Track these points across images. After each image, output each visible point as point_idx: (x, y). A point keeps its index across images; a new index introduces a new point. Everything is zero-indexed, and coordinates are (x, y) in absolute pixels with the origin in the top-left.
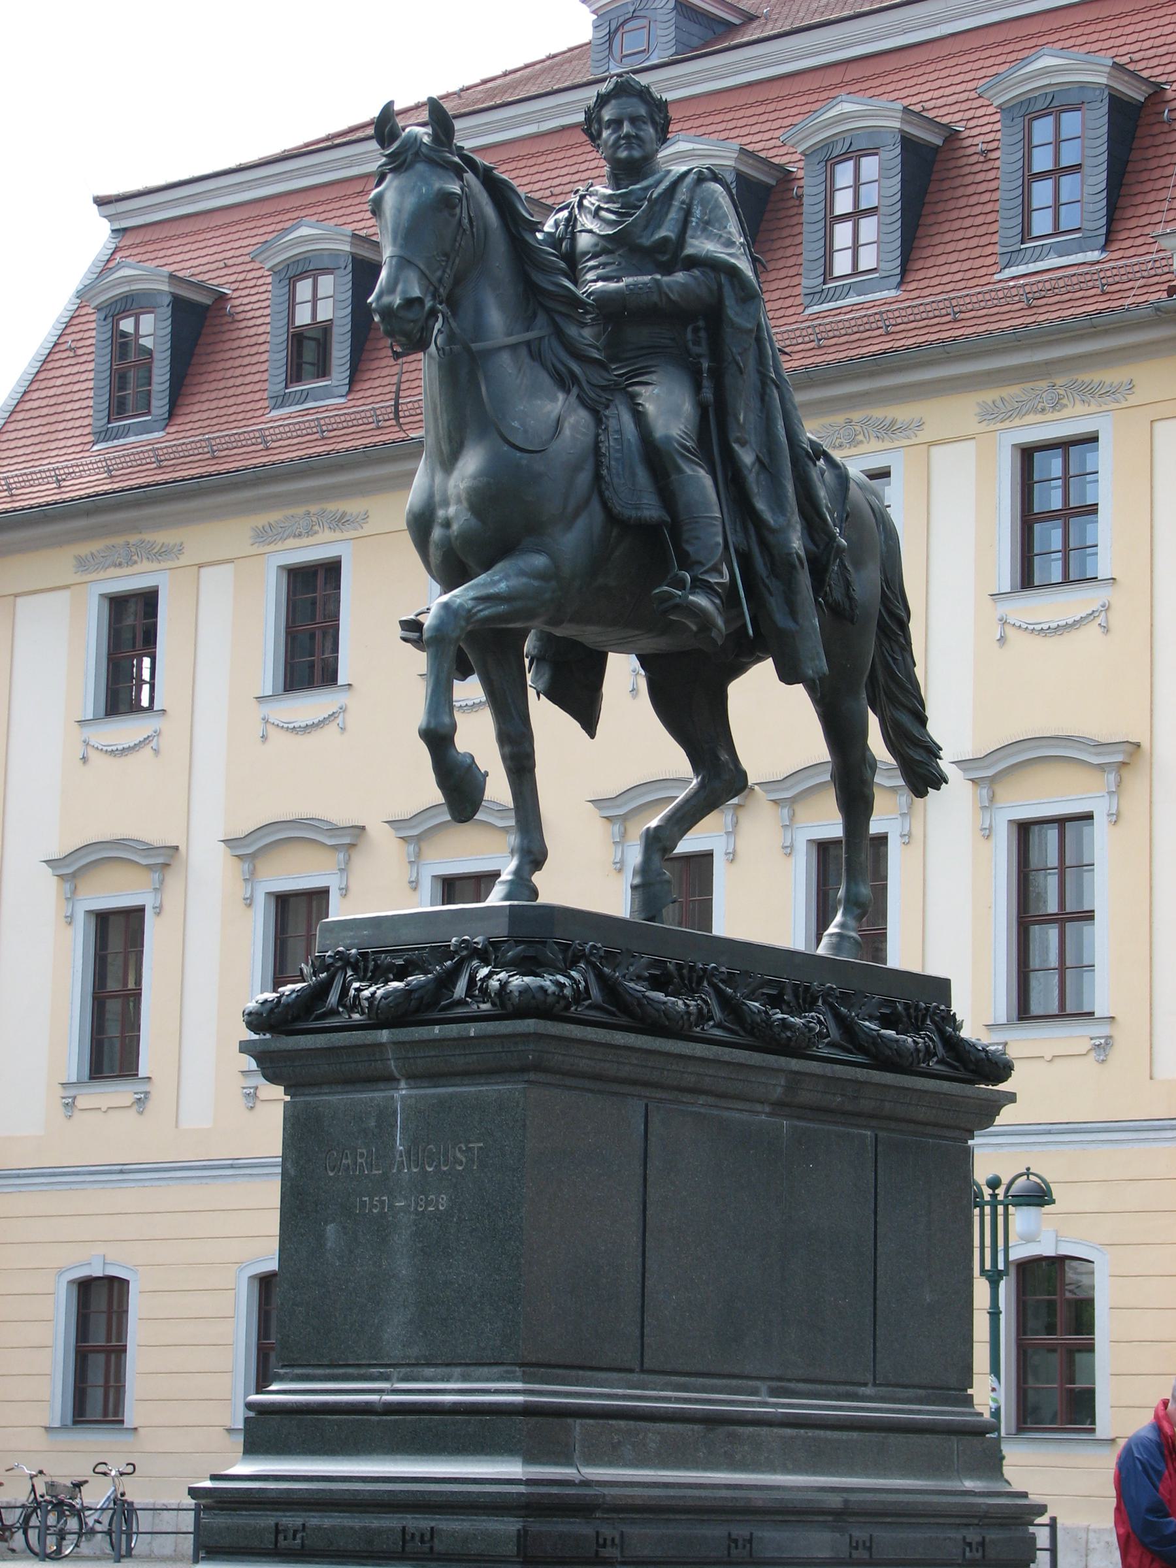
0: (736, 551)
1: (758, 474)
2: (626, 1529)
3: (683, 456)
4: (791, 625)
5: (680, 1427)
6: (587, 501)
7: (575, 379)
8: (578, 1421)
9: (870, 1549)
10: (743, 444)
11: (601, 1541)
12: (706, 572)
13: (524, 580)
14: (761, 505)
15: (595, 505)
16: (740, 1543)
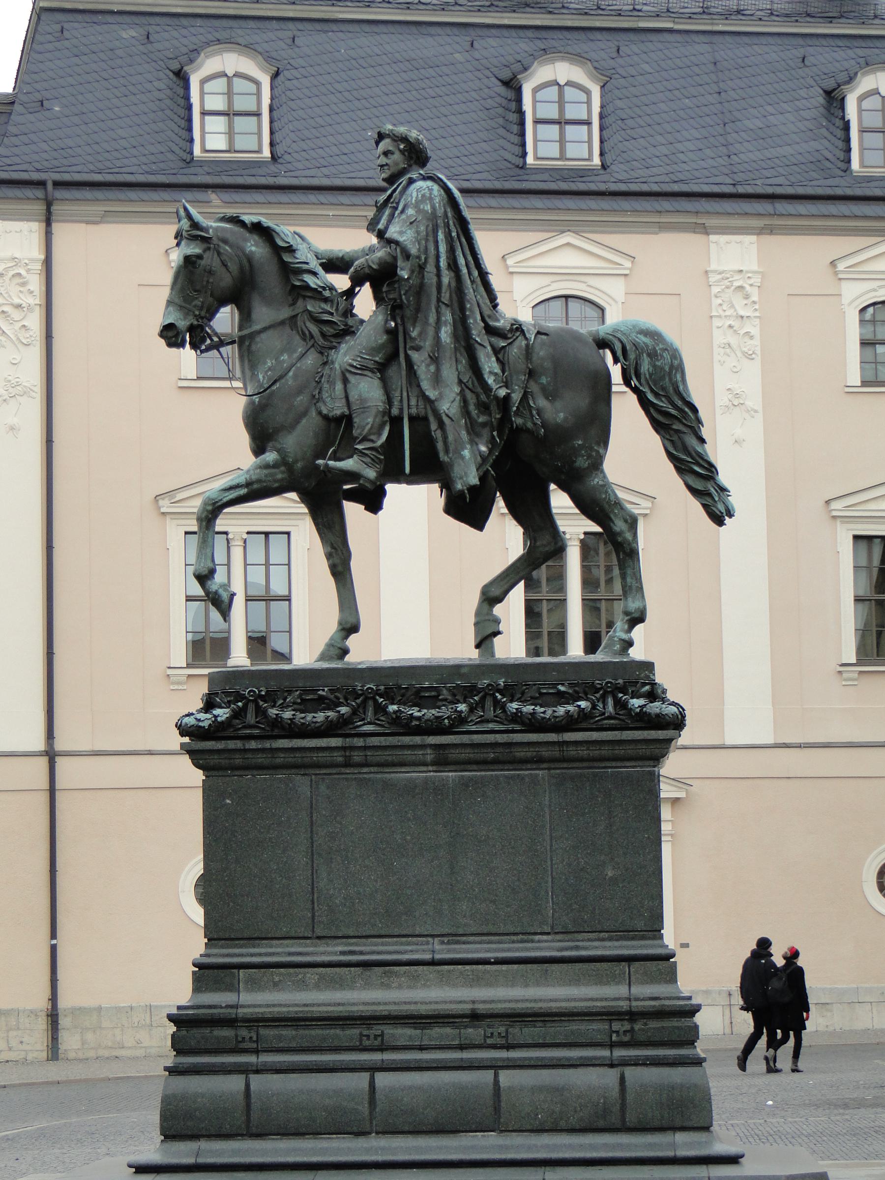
0: (412, 419)
1: (428, 366)
2: (262, 1031)
3: (350, 372)
4: (446, 459)
5: (337, 970)
6: (305, 413)
7: (312, 337)
8: (241, 971)
9: (506, 1037)
10: (417, 349)
11: (240, 1039)
12: (359, 443)
13: (265, 471)
14: (425, 385)
15: (313, 413)
16: (372, 1037)
